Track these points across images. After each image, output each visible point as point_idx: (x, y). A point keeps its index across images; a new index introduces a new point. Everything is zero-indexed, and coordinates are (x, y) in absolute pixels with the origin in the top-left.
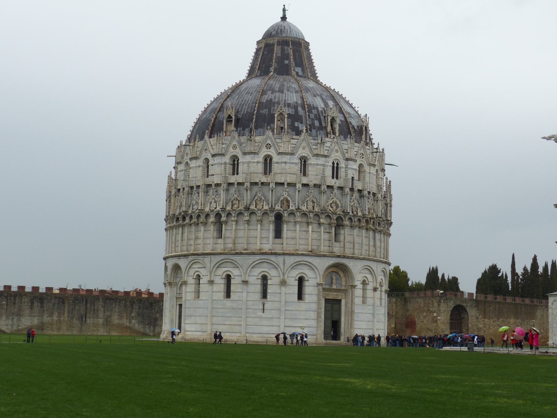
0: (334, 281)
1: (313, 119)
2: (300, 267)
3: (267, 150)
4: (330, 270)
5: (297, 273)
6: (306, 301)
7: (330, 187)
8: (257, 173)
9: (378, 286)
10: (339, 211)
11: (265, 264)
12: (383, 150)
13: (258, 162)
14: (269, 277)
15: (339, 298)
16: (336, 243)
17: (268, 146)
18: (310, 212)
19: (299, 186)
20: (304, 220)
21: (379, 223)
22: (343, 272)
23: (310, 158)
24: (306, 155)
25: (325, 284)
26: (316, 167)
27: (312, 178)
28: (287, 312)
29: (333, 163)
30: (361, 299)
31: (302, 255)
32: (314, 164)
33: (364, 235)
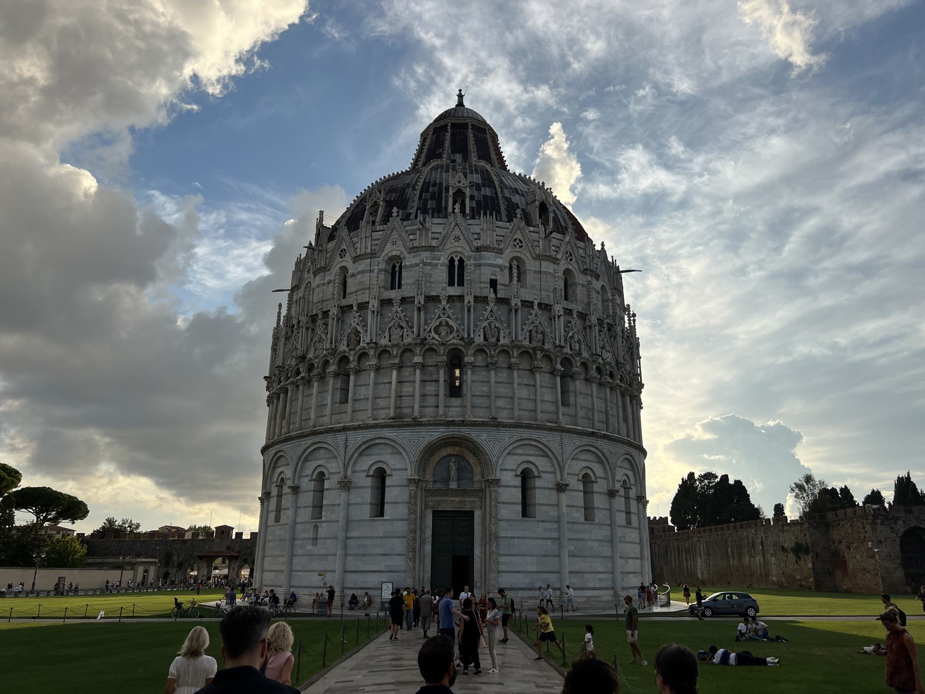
0: (453, 473)
2: (375, 450)
5: (370, 463)
6: (386, 517)
7: (432, 299)
8: (326, 300)
11: (322, 451)
12: (603, 245)
13: (329, 282)
14: (327, 476)
15: (467, 508)
16: (453, 399)
17: (343, 253)
18: (394, 346)
19: (374, 304)
20: (387, 362)
21: (566, 361)
22: (474, 454)
25: (434, 482)
26: (413, 269)
27: (408, 289)
28: (351, 542)
29: (452, 261)
30: (519, 508)
31: (376, 426)
32: (412, 266)
33: (516, 380)
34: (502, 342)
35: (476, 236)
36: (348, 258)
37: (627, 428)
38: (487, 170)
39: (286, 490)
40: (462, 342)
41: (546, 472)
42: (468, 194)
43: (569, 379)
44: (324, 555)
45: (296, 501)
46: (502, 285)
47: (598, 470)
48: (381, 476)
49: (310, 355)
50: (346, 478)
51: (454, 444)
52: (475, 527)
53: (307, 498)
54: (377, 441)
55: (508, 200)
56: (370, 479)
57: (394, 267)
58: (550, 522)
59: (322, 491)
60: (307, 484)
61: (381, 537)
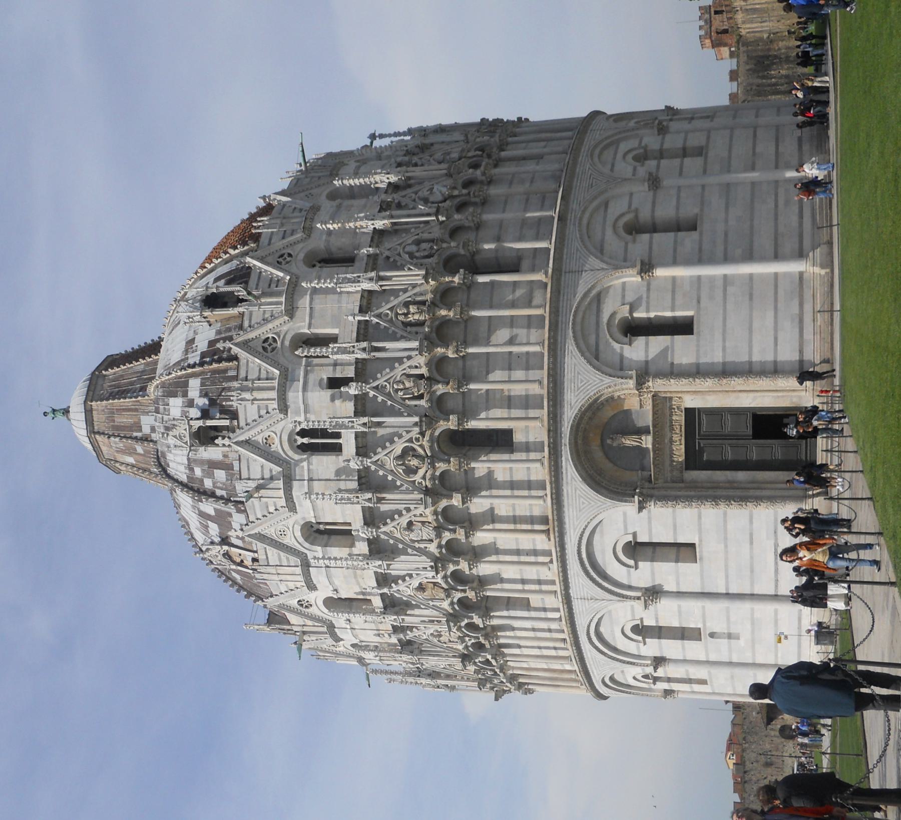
1: (214, 483)
3: (314, 607)
4: (599, 455)
6: (695, 540)
9: (642, 171)
10: (424, 446)
11: (602, 629)
14: (639, 622)
15: (679, 418)
18: (439, 536)
19: (377, 565)
21: (450, 265)
23: (304, 518)
24: (298, 528)
27: (351, 515)
29: (303, 448)
34: (424, 371)
35: (263, 412)
36: (311, 597)
37: (550, 154)
38: (163, 385)
39: (660, 672)
40: (428, 433)
41: (623, 297)
42: (200, 423)
43: (477, 257)
44: (753, 623)
45: (676, 661)
46: (334, 370)
47: (617, 208)
48: (637, 550)
49: (460, 647)
50: (639, 598)
51: (586, 439)
52: (709, 405)
53: (670, 648)
54: (584, 556)
55: (203, 355)
56: (641, 564)
57: (319, 531)
58: (699, 288)
59: (660, 627)
60: (652, 647)
61: (726, 546)
